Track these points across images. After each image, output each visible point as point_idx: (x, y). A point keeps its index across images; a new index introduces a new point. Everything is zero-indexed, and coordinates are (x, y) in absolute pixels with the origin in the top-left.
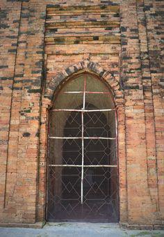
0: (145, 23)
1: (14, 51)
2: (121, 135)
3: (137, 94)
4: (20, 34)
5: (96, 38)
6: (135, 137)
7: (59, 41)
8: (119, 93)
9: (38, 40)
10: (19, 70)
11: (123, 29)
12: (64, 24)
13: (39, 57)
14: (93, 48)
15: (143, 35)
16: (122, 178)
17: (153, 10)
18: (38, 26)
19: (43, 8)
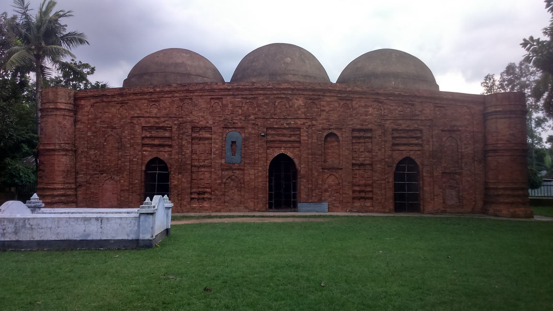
2: (421, 182)
4: (382, 141)
5: (411, 144)
8: (421, 167)
10: (383, 157)
14: (410, 148)
15: (431, 143)
18: (389, 138)
19: (391, 130)
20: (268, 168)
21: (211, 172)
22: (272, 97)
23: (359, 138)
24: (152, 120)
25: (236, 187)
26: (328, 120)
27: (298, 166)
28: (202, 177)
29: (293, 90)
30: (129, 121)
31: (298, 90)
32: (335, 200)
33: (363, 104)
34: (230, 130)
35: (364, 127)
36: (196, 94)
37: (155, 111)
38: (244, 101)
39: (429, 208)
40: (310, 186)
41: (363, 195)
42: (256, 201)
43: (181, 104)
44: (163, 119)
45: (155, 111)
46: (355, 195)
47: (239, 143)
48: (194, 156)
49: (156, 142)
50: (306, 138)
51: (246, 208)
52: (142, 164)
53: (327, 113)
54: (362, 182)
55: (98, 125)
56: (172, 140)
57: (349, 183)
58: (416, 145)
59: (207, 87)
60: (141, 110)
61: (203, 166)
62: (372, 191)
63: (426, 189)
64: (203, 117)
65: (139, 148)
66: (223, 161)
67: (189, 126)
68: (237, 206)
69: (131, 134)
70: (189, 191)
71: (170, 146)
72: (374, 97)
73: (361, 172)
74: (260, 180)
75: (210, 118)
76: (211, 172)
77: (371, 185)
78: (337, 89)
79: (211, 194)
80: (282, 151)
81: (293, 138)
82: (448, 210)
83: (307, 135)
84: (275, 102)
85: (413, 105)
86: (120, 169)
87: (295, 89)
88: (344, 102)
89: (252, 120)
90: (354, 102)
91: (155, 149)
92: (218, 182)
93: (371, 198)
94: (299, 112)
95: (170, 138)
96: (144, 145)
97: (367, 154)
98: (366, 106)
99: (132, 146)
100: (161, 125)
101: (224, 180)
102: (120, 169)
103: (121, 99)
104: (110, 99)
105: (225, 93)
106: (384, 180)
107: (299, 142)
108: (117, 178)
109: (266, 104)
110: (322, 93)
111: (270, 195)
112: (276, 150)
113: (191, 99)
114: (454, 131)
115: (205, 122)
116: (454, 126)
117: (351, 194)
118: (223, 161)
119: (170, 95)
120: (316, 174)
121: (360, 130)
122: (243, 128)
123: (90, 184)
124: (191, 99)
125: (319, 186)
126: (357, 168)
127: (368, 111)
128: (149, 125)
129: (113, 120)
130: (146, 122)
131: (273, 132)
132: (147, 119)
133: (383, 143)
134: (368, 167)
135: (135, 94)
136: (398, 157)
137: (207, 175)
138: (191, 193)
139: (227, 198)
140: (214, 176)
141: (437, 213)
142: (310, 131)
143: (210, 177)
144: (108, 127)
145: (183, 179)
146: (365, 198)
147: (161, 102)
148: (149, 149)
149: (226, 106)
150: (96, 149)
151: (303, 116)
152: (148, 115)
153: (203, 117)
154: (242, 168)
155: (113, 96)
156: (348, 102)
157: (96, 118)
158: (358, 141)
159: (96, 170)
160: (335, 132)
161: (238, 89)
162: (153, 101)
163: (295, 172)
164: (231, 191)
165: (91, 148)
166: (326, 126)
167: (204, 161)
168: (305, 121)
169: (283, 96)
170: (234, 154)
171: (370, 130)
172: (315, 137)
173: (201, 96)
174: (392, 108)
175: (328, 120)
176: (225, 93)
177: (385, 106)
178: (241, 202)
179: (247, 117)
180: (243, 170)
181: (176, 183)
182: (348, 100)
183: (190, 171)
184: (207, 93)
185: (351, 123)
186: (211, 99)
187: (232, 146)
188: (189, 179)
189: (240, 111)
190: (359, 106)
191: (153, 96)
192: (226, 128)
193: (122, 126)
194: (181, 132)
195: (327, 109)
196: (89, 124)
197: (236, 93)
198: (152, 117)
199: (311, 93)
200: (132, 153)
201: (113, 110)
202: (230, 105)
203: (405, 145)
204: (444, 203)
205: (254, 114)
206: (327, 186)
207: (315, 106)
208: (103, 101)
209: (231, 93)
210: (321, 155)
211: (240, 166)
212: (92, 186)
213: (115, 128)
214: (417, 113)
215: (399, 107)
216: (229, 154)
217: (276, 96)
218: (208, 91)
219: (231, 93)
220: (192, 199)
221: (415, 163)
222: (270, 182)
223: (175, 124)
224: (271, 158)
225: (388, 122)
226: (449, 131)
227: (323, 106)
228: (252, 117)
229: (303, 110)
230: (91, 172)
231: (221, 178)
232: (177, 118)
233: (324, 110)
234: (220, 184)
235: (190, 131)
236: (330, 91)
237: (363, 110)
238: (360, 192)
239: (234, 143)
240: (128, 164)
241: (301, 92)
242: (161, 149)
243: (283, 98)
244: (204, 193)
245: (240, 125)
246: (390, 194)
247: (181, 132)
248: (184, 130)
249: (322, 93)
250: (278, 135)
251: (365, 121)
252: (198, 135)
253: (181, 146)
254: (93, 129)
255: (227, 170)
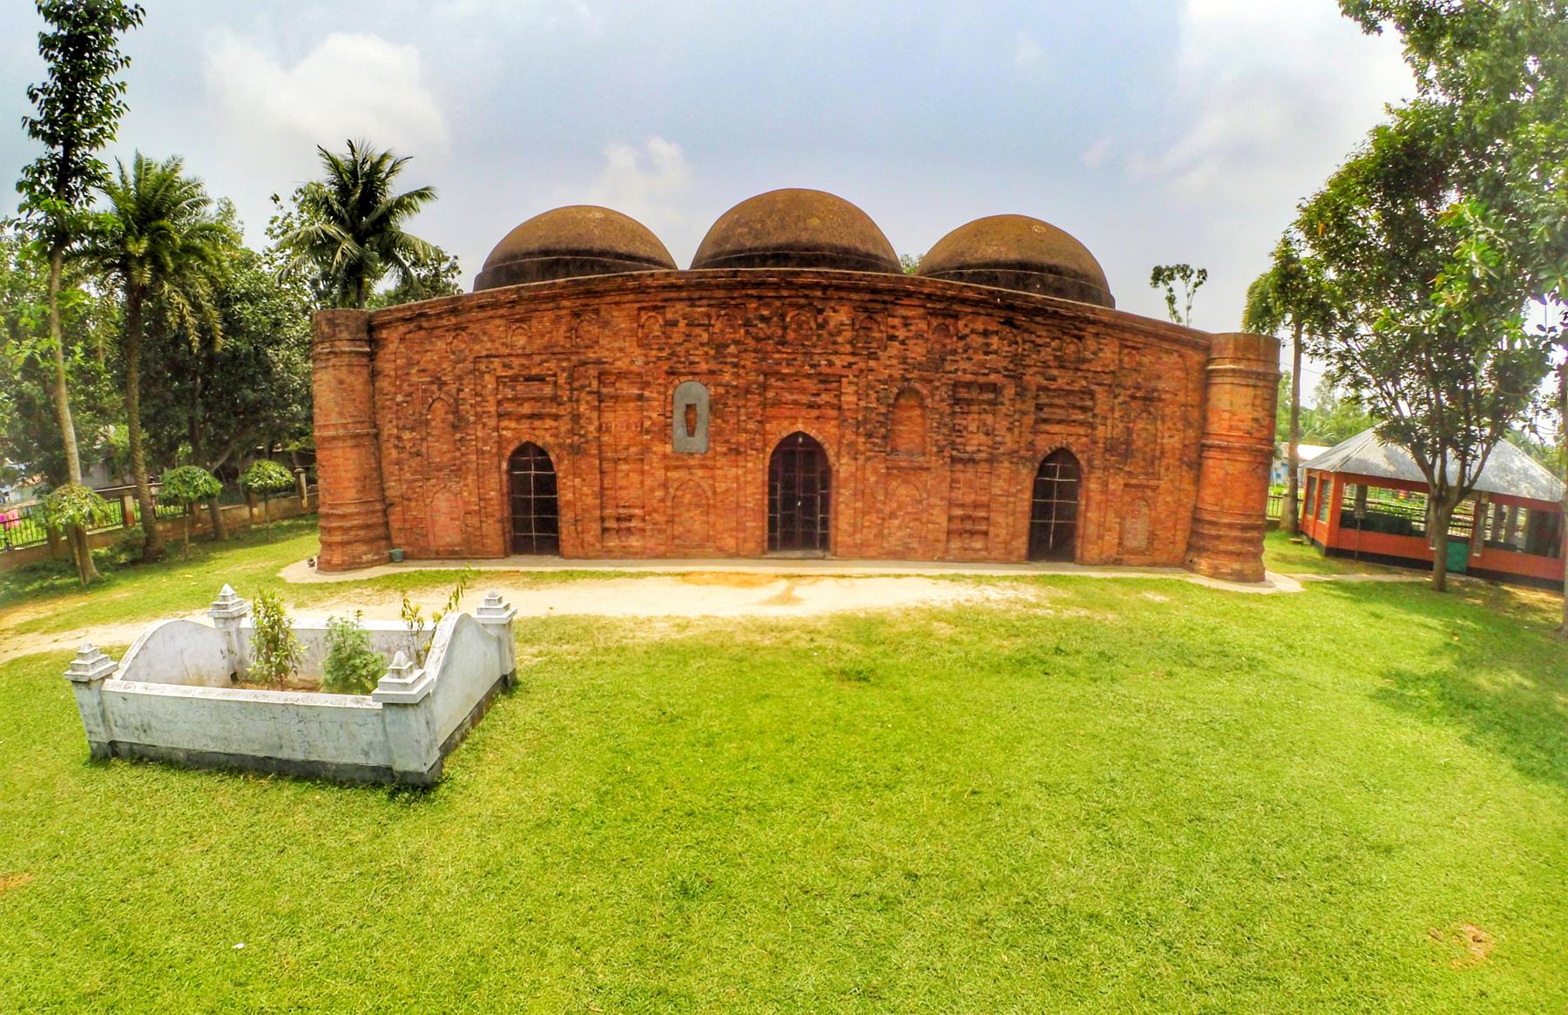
0: (1112, 410)
1: (1009, 429)
3: (1099, 473)
6: (1093, 504)
7: (1045, 421)
8: (1086, 469)
9: (1029, 420)
10: (1016, 447)
11: (1095, 416)
12: (1051, 406)
13: (1030, 437)
14: (1071, 429)
15: (1109, 422)
16: (1081, 531)
17: (1121, 399)
18: (1029, 406)
20: (767, 463)
21: (643, 472)
22: (778, 303)
23: (969, 402)
24: (516, 362)
25: (698, 506)
26: (904, 360)
27: (832, 459)
28: (622, 483)
29: (825, 288)
30: (471, 366)
31: (838, 288)
32: (910, 536)
33: (980, 326)
34: (683, 379)
35: (982, 380)
36: (608, 299)
37: (521, 341)
38: (713, 311)
39: (1092, 551)
40: (859, 505)
41: (968, 526)
42: (741, 535)
43: (574, 323)
44: (537, 359)
45: (521, 341)
46: (953, 527)
47: (703, 410)
48: (605, 438)
49: (527, 409)
50: (854, 399)
51: (720, 549)
52: (499, 455)
53: (903, 343)
54: (970, 498)
55: (415, 379)
56: (560, 404)
57: (942, 499)
58: (1082, 424)
59: (631, 284)
60: (493, 341)
61: (626, 460)
62: (987, 519)
63: (1092, 515)
64: (621, 350)
65: (492, 423)
66: (668, 449)
67: (593, 372)
68: (700, 546)
69: (477, 395)
70: (597, 513)
71: (556, 417)
72: (1003, 314)
73: (970, 475)
74: (750, 489)
75: (638, 351)
76: (643, 472)
77: (987, 507)
78: (926, 290)
79: (644, 520)
80: (800, 427)
81: (825, 397)
82: (1126, 557)
83: (856, 392)
84: (783, 317)
85: (1080, 338)
86: (459, 469)
87: (830, 286)
88: (940, 320)
89: (734, 356)
90: (961, 324)
91: (525, 425)
92: (659, 493)
93: (986, 533)
94: (840, 339)
95: (555, 399)
96: (500, 416)
97: (982, 437)
98: (986, 333)
99: (478, 416)
100: (534, 372)
101: (672, 491)
102: (459, 469)
103: (454, 320)
104: (433, 323)
105: (673, 295)
106: (1015, 495)
107: (840, 408)
108: (455, 487)
109: (763, 319)
110: (891, 298)
111: (772, 523)
112: (786, 423)
113: (597, 311)
114: (1151, 400)
115: (627, 360)
116: (1154, 390)
117: (945, 524)
118: (668, 449)
119: (551, 305)
120: (873, 479)
121: (968, 385)
122: (712, 372)
123: (409, 500)
124: (597, 311)
125: (879, 505)
126: (960, 467)
127: (988, 345)
128: (510, 373)
129: (439, 365)
130: (505, 366)
131: (779, 384)
132: (507, 360)
133: (1017, 416)
134: (984, 467)
135: (481, 307)
136: (1044, 445)
137: (635, 478)
138: (603, 519)
139: (679, 530)
140: (649, 482)
141: (1106, 563)
142: (863, 382)
143: (642, 483)
144: (432, 383)
145: (585, 489)
146: (972, 533)
147: (534, 322)
148: (513, 425)
149: (675, 324)
150: (412, 429)
151: (848, 348)
152: (507, 351)
153: (621, 350)
154: (709, 463)
155: (439, 316)
156: (949, 321)
157: (410, 365)
158: (966, 409)
159: (416, 472)
160: (918, 386)
161: (699, 286)
162: (517, 321)
163: (826, 475)
164: (687, 515)
165: (404, 428)
166: (897, 373)
167: (627, 448)
168: (852, 359)
169: (802, 301)
170: (691, 433)
171: (994, 388)
172: (873, 395)
173: (616, 303)
174: (1039, 341)
175: (904, 360)
176: (673, 295)
177: (1026, 336)
178: (708, 538)
179: (720, 347)
180: (711, 468)
181: (569, 496)
182: (945, 316)
183: (596, 471)
184: (631, 297)
185: (952, 368)
186: (640, 309)
187: (686, 413)
188: (596, 489)
189: (705, 336)
190: (973, 331)
191: (518, 309)
192: (673, 373)
193: (460, 378)
194: (576, 384)
195: (901, 333)
196: (397, 377)
197: (697, 295)
198: (517, 356)
199: (867, 297)
200: (479, 434)
201: (441, 345)
202: (682, 323)
203: (1059, 422)
204: (1120, 544)
205: (736, 342)
206: (895, 505)
207: (875, 327)
208: (420, 328)
209: (684, 294)
210: (884, 437)
211: (705, 459)
212: (413, 504)
213: (445, 383)
214: (1089, 355)
215: (1053, 339)
216: (679, 431)
217: (787, 301)
218: (633, 290)
219: (684, 294)
220: (605, 530)
221: (1077, 462)
222: (772, 491)
223: (563, 370)
224: (774, 442)
225: (1031, 371)
226: (1144, 399)
227: (893, 327)
228: (732, 349)
229: (848, 334)
230: (408, 476)
231: (665, 485)
232: (567, 355)
233: (892, 338)
234: (663, 500)
235: (595, 384)
236: (909, 294)
237: (981, 340)
238: (963, 519)
239: (690, 408)
240: (473, 457)
241: (843, 294)
242: (537, 423)
243: (801, 307)
244: (630, 518)
245: (704, 367)
246: (1024, 524)
247: (576, 384)
248: (581, 382)
249: (891, 298)
250: (791, 390)
251: (982, 365)
252: (611, 390)
253: (576, 418)
254: (405, 387)
255: (677, 468)
